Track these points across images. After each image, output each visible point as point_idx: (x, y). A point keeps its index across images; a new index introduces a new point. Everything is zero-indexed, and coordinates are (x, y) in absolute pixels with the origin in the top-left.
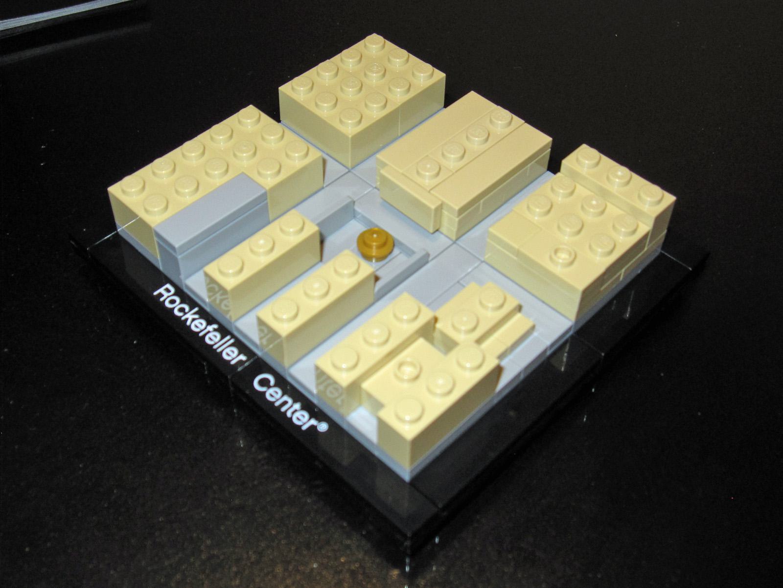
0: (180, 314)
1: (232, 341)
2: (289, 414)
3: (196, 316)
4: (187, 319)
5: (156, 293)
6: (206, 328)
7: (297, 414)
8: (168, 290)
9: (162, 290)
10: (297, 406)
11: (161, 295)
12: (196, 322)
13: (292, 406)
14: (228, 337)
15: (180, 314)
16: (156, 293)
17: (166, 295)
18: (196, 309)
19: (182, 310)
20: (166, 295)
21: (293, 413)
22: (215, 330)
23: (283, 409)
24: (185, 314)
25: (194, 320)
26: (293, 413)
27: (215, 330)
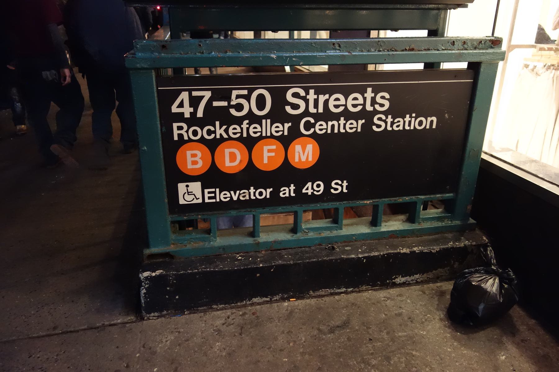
0: (213, 136)
1: (269, 121)
2: (342, 130)
3: (224, 127)
4: (221, 135)
5: (176, 138)
6: (242, 129)
7: (348, 126)
8: (180, 128)
9: (176, 132)
10: (342, 121)
11: (180, 136)
12: (231, 131)
13: (339, 125)
14: (264, 121)
15: (213, 136)
16: (176, 138)
17: (183, 132)
19: (209, 132)
21: (344, 128)
22: (250, 124)
23: (336, 131)
24: (214, 132)
25: (226, 131)
26: (344, 128)
27: (250, 124)
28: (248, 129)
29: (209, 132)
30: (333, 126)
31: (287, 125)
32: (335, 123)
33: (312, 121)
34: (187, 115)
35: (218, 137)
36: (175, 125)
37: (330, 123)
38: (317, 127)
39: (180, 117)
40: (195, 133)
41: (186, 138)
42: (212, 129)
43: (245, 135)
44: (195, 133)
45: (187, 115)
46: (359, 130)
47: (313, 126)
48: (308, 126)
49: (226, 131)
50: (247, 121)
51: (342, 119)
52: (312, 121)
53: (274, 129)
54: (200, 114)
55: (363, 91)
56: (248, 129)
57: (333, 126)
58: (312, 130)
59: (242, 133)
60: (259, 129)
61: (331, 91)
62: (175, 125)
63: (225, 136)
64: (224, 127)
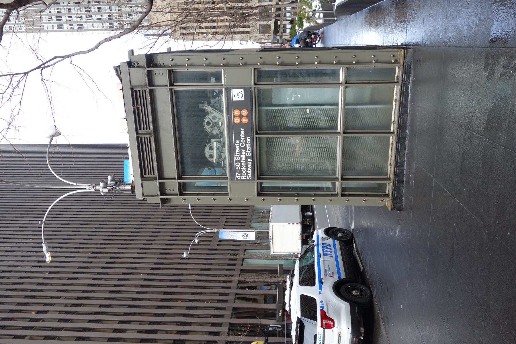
1: (241, 155)
2: (244, 135)
3: (243, 167)
7: (243, 133)
8: (243, 177)
9: (244, 178)
11: (245, 177)
12: (244, 165)
15: (245, 170)
17: (244, 177)
18: (242, 168)
20: (244, 177)
22: (242, 160)
24: (244, 169)
25: (244, 166)
27: (242, 160)
28: (243, 161)
29: (244, 170)
30: (243, 138)
31: (242, 150)
32: (242, 137)
33: (241, 144)
34: (240, 177)
35: (245, 168)
36: (242, 178)
37: (242, 138)
38: (243, 142)
39: (240, 178)
40: (244, 174)
41: (245, 176)
42: (243, 170)
43: (245, 161)
44: (244, 174)
45: (240, 177)
46: (244, 130)
47: (242, 143)
48: (242, 145)
49: (244, 166)
50: (241, 161)
51: (240, 135)
52: (241, 144)
53: (243, 154)
54: (240, 174)
55: (236, 146)
56: (243, 161)
57: (243, 138)
58: (244, 143)
59: (244, 162)
60: (243, 158)
61: (235, 152)
62: (242, 178)
63: (245, 166)
64: (243, 167)
